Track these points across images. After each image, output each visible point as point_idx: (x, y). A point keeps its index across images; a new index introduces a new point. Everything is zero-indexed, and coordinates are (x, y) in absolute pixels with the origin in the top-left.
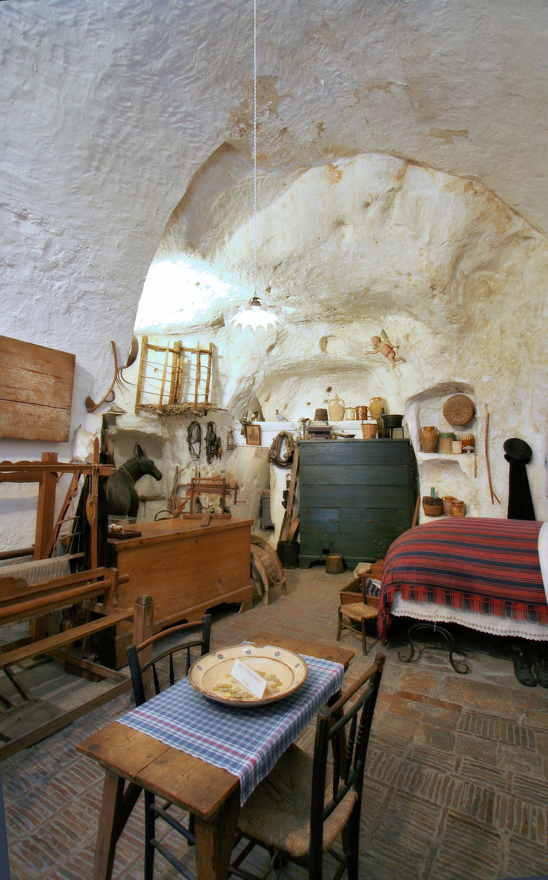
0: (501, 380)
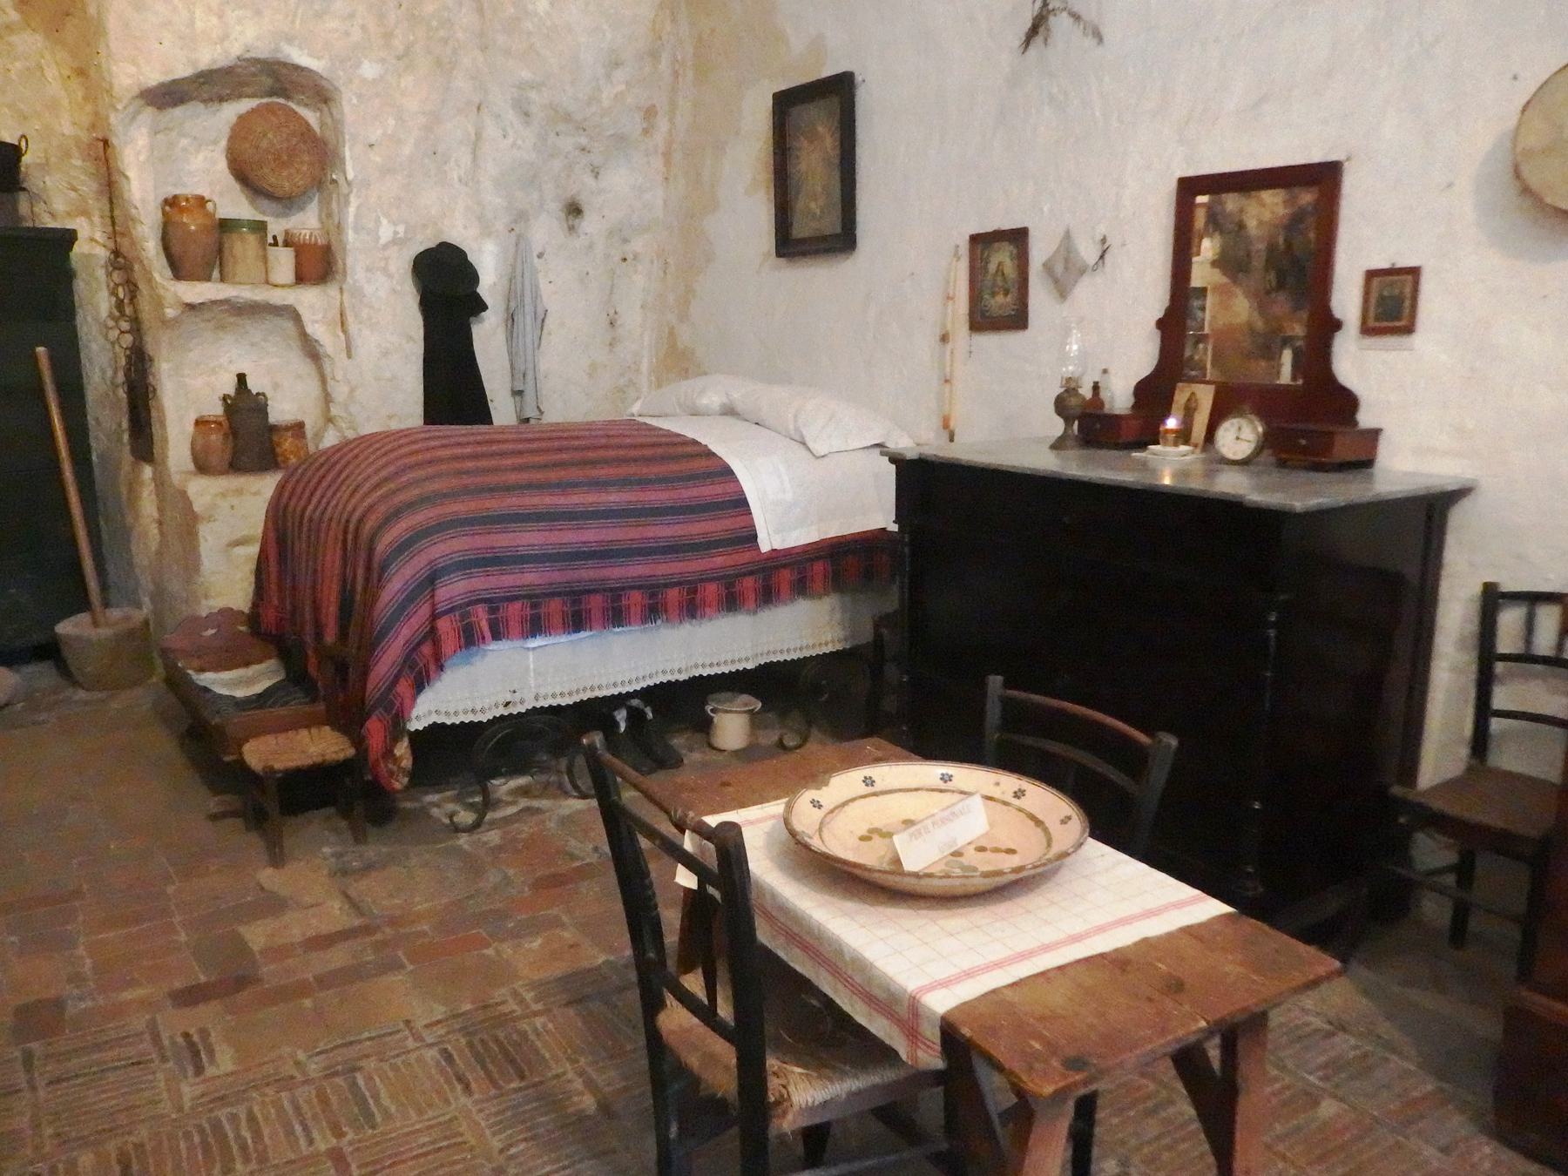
0: (407, 81)
